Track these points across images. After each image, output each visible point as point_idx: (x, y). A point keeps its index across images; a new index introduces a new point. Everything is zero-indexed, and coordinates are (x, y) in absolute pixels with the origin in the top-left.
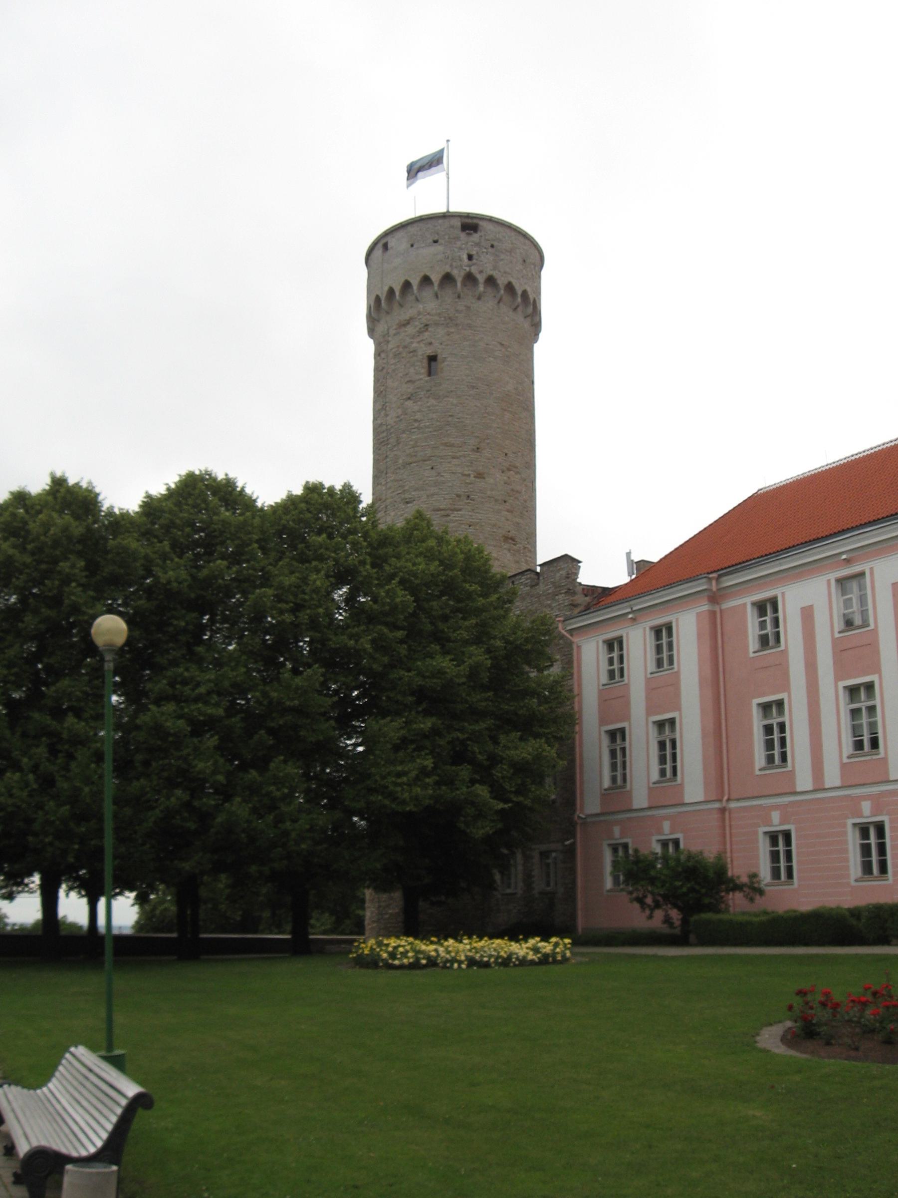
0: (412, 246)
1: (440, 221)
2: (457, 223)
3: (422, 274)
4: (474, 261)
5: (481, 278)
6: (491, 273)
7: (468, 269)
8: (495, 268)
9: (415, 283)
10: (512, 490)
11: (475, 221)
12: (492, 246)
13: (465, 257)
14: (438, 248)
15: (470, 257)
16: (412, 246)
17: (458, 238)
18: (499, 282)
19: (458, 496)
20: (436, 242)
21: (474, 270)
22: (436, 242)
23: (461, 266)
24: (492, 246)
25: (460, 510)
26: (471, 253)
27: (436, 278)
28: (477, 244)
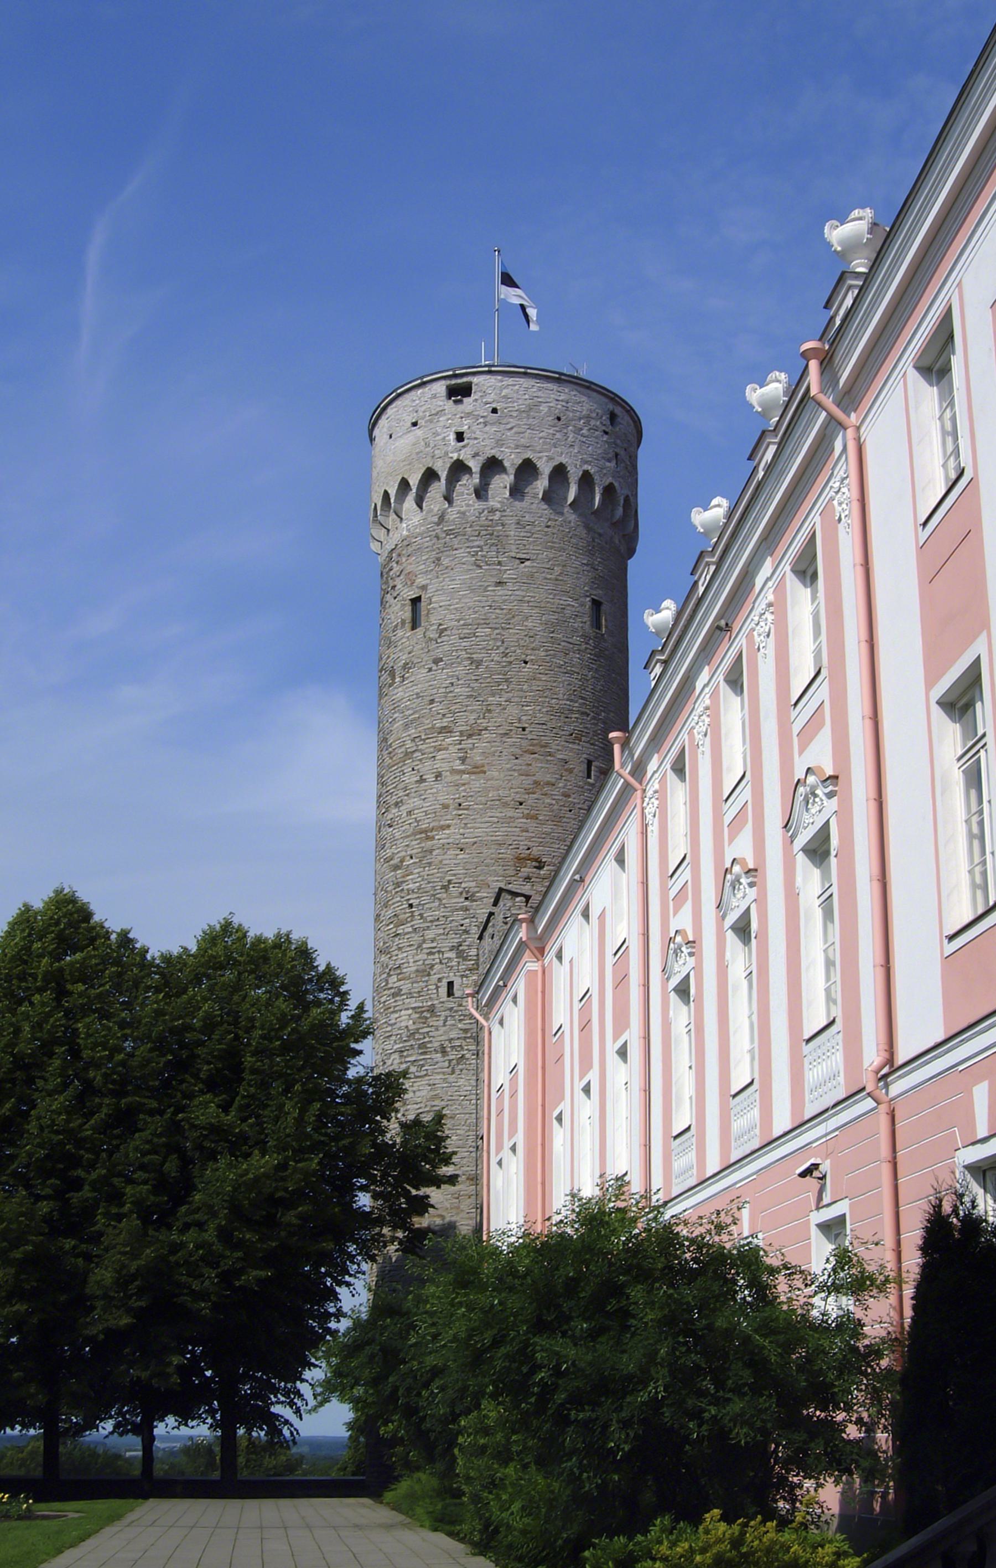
0: (391, 437)
1: (420, 391)
2: (440, 388)
3: (400, 478)
4: (466, 441)
5: (475, 465)
6: (493, 452)
7: (455, 456)
8: (499, 443)
9: (393, 493)
10: (536, 783)
11: (465, 380)
12: (494, 411)
13: (452, 437)
14: (418, 432)
15: (460, 437)
16: (391, 437)
17: (440, 412)
18: (506, 464)
19: (445, 807)
20: (415, 424)
21: (465, 455)
22: (415, 424)
23: (446, 453)
24: (494, 411)
25: (448, 826)
26: (460, 430)
27: (414, 481)
28: (469, 415)
